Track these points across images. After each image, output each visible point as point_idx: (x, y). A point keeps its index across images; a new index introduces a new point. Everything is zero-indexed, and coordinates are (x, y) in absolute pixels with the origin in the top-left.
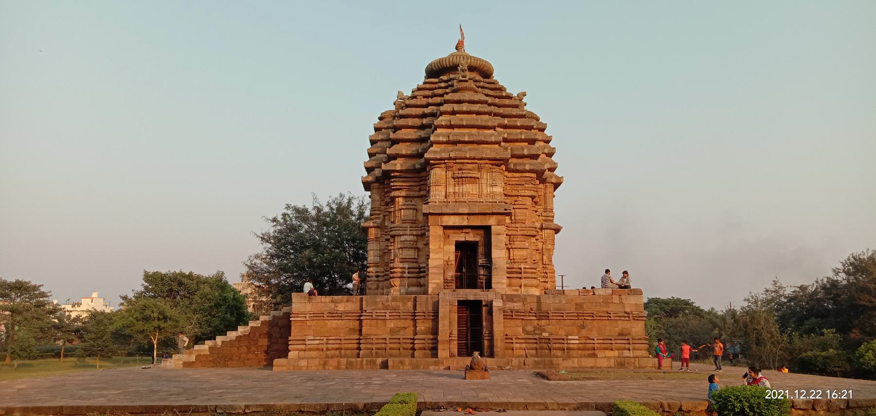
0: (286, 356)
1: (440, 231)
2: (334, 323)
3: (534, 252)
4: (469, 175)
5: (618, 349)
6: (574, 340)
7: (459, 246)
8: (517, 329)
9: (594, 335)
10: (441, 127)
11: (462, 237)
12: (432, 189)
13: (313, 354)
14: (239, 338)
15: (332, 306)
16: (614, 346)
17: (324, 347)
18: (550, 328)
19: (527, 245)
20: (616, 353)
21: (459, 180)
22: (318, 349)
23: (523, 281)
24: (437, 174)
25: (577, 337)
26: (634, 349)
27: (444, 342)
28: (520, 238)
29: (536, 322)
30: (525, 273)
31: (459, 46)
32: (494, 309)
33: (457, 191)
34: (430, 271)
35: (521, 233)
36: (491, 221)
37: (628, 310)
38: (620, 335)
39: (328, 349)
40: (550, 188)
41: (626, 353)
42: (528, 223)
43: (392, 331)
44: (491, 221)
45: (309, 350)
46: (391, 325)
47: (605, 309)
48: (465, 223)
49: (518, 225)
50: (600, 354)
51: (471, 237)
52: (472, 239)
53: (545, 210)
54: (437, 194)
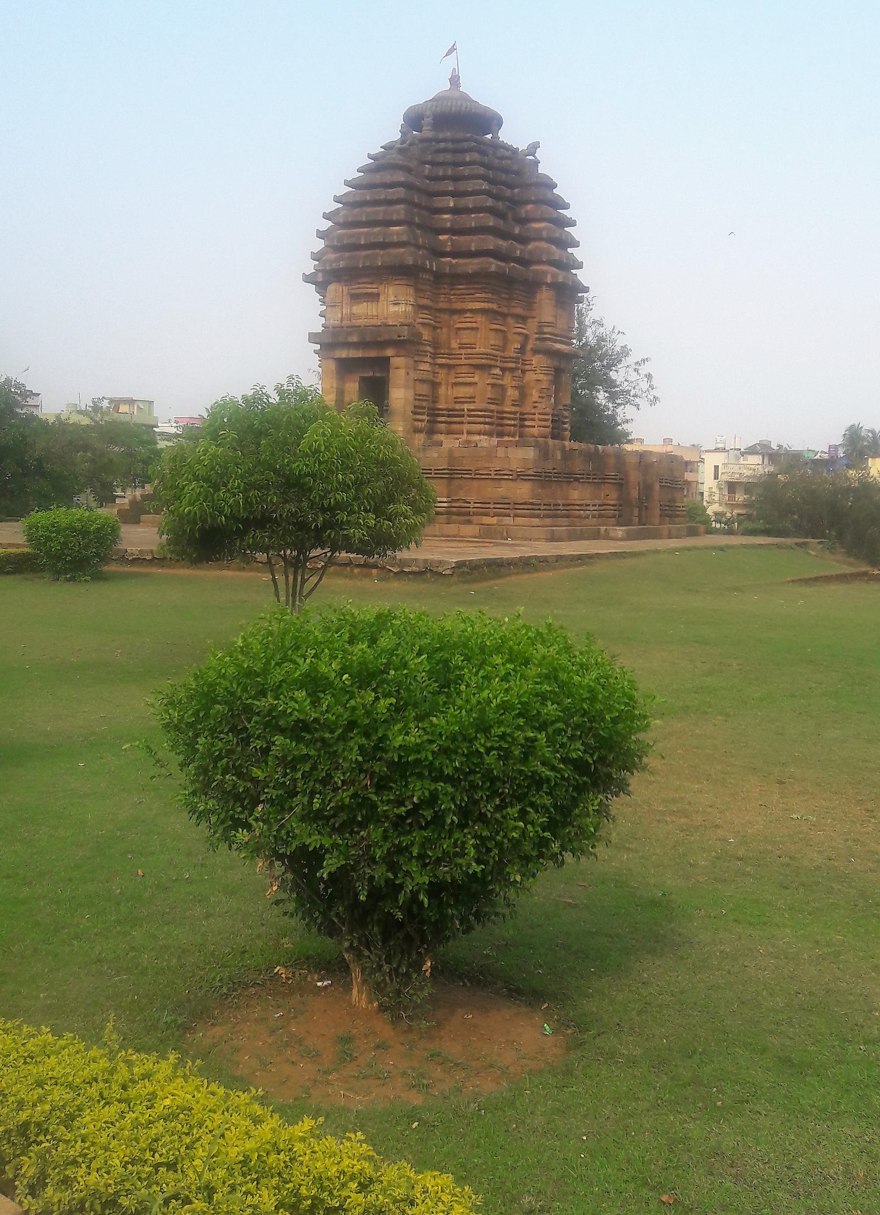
3: (489, 388)
4: (365, 291)
9: (472, 498)
19: (476, 379)
20: (494, 520)
21: (356, 298)
23: (466, 427)
25: (445, 499)
26: (516, 516)
28: (464, 369)
30: (469, 416)
31: (455, 80)
33: (354, 311)
35: (467, 361)
36: (389, 352)
37: (514, 466)
41: (508, 520)
44: (389, 352)
47: (487, 465)
48: (359, 354)
49: (463, 351)
52: (378, 375)
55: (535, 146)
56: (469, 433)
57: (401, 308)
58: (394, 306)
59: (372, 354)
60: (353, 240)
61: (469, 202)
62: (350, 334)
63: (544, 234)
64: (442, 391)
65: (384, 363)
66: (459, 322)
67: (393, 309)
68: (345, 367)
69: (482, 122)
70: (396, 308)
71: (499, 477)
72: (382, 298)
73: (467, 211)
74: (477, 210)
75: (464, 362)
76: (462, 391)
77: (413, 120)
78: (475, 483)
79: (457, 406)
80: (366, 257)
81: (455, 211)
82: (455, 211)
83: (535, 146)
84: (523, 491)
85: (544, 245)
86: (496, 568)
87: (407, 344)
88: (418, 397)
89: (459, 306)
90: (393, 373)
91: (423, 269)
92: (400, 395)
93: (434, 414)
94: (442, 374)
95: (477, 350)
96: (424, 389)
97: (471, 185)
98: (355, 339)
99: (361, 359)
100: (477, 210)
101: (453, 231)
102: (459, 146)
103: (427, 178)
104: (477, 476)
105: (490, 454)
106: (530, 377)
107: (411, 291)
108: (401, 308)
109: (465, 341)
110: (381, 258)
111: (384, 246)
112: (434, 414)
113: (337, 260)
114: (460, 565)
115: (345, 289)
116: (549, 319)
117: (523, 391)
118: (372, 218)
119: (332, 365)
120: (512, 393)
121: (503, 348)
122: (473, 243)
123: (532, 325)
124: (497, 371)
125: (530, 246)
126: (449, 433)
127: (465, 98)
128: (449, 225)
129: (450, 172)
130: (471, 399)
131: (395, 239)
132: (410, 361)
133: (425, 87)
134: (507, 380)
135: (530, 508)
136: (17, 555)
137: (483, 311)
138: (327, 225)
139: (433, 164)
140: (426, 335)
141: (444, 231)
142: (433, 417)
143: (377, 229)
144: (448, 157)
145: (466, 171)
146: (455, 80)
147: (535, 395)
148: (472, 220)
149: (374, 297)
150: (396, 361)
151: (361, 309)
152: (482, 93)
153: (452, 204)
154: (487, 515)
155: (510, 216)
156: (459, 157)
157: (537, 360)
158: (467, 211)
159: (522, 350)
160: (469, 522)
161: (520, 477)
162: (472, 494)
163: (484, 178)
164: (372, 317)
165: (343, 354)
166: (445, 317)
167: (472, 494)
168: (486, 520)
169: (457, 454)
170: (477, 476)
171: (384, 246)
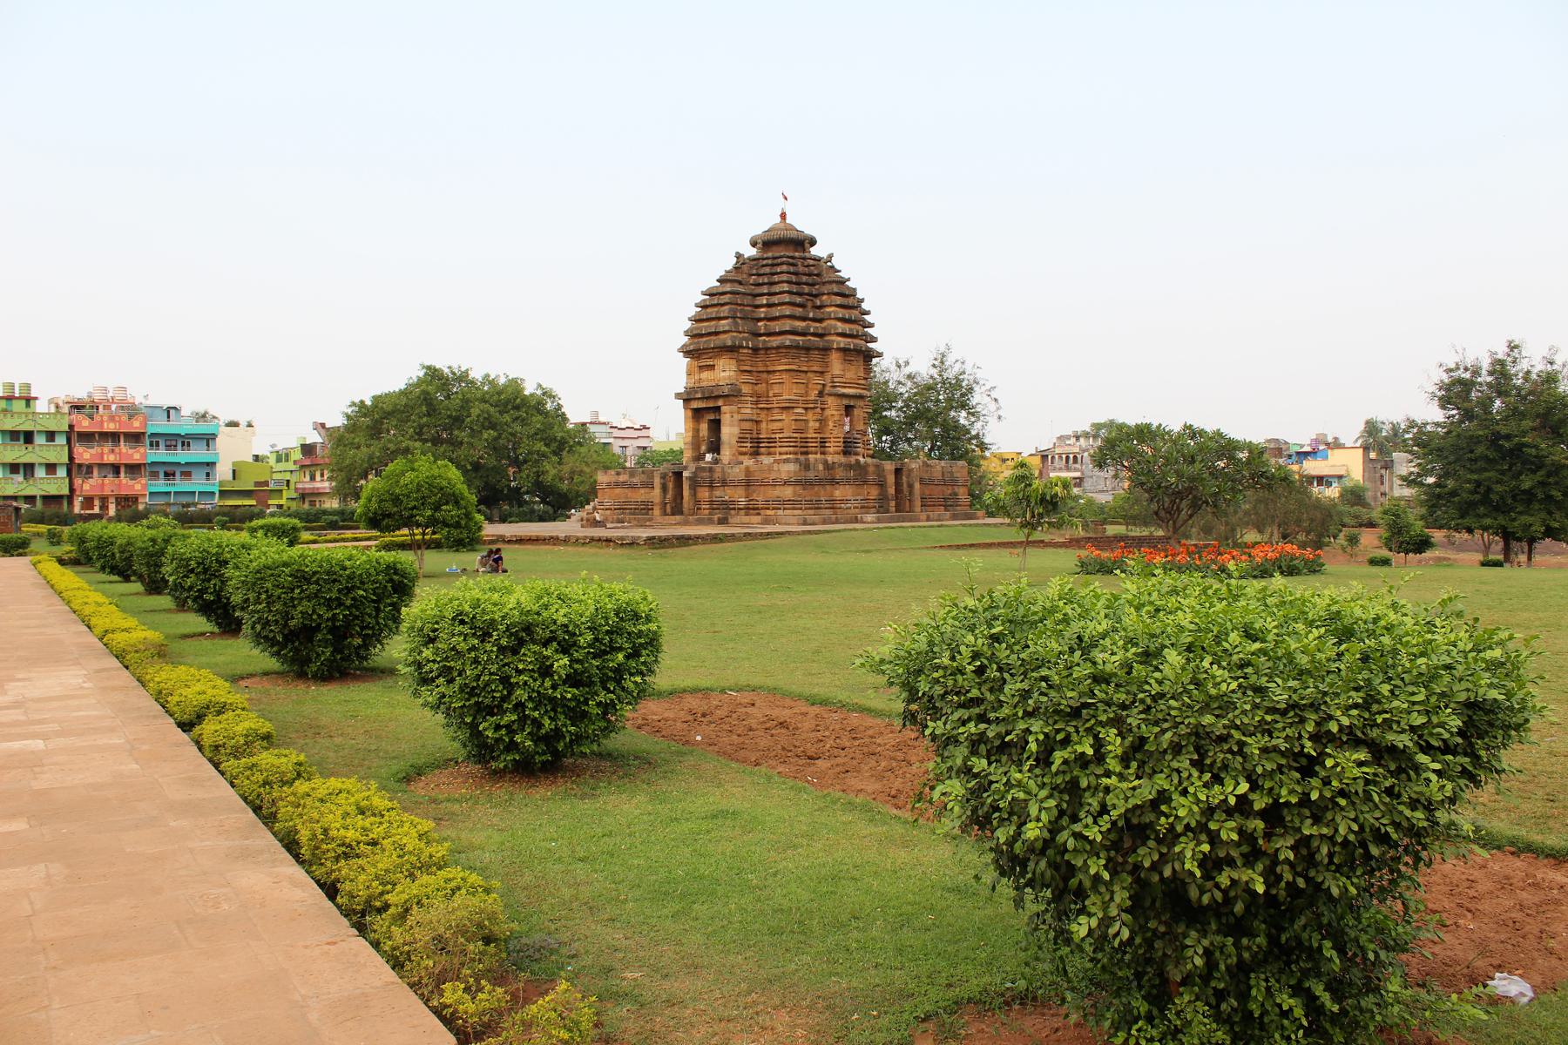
2: (618, 491)
6: (743, 502)
18: (727, 494)
31: (783, 216)
36: (720, 403)
41: (780, 512)
44: (720, 403)
55: (831, 256)
58: (724, 372)
64: (763, 425)
68: (697, 414)
69: (802, 243)
81: (769, 306)
82: (769, 306)
83: (831, 256)
84: (788, 492)
85: (833, 322)
86: (684, 541)
87: (733, 395)
88: (743, 431)
92: (729, 432)
93: (757, 442)
94: (763, 416)
96: (747, 425)
97: (777, 289)
99: (703, 407)
105: (770, 469)
106: (828, 412)
110: (713, 342)
111: (717, 333)
112: (757, 442)
114: (650, 539)
116: (837, 372)
117: (823, 421)
119: (690, 413)
120: (813, 425)
121: (807, 394)
122: (777, 326)
123: (828, 377)
125: (824, 324)
130: (781, 430)
132: (734, 408)
133: (764, 222)
134: (810, 416)
135: (793, 504)
140: (745, 389)
141: (760, 320)
142: (755, 445)
144: (767, 270)
145: (776, 278)
146: (783, 216)
148: (776, 312)
149: (712, 367)
150: (724, 409)
151: (705, 375)
152: (802, 223)
155: (809, 304)
157: (830, 401)
159: (821, 394)
162: (760, 496)
163: (789, 282)
165: (695, 405)
166: (765, 376)
167: (760, 496)
168: (769, 512)
171: (717, 333)
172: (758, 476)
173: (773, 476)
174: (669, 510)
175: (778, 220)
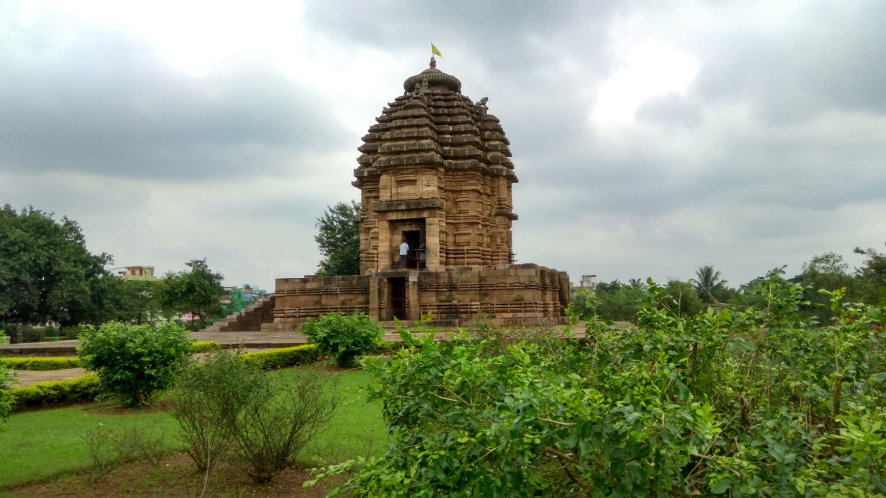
0: (272, 321)
1: (386, 225)
5: (512, 311)
7: (405, 233)
8: (431, 298)
9: (495, 301)
10: (386, 140)
11: (408, 228)
12: (381, 191)
13: (291, 320)
14: (256, 310)
15: (302, 285)
16: (509, 310)
17: (297, 315)
18: (458, 299)
19: (470, 231)
20: (510, 315)
21: (400, 183)
22: (295, 317)
23: (466, 260)
24: (384, 179)
26: (526, 311)
27: (374, 309)
29: (448, 293)
31: (433, 64)
32: (410, 284)
34: (380, 256)
36: (425, 215)
37: (522, 281)
38: (515, 300)
39: (300, 317)
40: (503, 182)
41: (519, 315)
42: (471, 213)
43: (343, 303)
44: (425, 215)
45: (288, 317)
46: (342, 298)
47: (503, 281)
48: (405, 217)
50: (497, 315)
51: (414, 228)
52: (414, 229)
53: (499, 200)
54: (385, 196)
55: (485, 100)
56: (468, 264)
57: (431, 189)
59: (414, 216)
60: (399, 149)
61: (462, 128)
62: (400, 204)
63: (499, 148)
65: (422, 222)
66: (464, 196)
67: (426, 189)
70: (428, 189)
71: (511, 289)
72: (418, 182)
73: (460, 133)
74: (466, 132)
75: (463, 221)
76: (461, 239)
77: (410, 85)
78: (496, 292)
79: (459, 248)
80: (408, 158)
82: (452, 133)
89: (458, 188)
90: (427, 228)
91: (442, 165)
92: (433, 241)
95: (470, 214)
98: (403, 207)
100: (466, 132)
101: (452, 145)
102: (448, 97)
103: (434, 115)
104: (497, 288)
107: (436, 178)
108: (431, 189)
109: (462, 209)
111: (417, 151)
113: (389, 161)
115: (393, 178)
118: (410, 135)
123: (495, 199)
124: (480, 226)
126: (455, 264)
127: (440, 72)
128: (450, 141)
129: (446, 111)
131: (426, 147)
136: (292, 353)
137: (474, 191)
138: (363, 143)
139: (435, 107)
141: (447, 144)
142: (450, 254)
143: (412, 142)
146: (433, 64)
147: (499, 241)
149: (413, 182)
150: (428, 220)
153: (451, 129)
154: (506, 312)
156: (450, 104)
158: (460, 133)
160: (494, 317)
161: (527, 287)
162: (494, 300)
164: (412, 194)
165: (394, 216)
169: (483, 275)
170: (497, 288)
171: (417, 151)
172: (490, 281)
173: (509, 281)
174: (384, 315)
175: (429, 67)
